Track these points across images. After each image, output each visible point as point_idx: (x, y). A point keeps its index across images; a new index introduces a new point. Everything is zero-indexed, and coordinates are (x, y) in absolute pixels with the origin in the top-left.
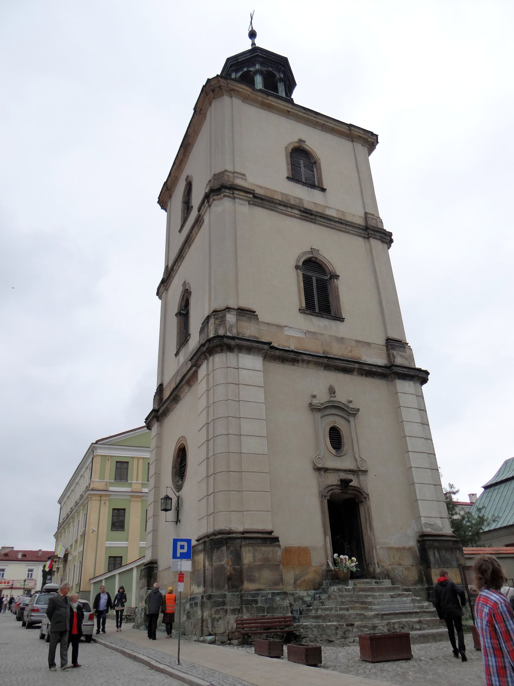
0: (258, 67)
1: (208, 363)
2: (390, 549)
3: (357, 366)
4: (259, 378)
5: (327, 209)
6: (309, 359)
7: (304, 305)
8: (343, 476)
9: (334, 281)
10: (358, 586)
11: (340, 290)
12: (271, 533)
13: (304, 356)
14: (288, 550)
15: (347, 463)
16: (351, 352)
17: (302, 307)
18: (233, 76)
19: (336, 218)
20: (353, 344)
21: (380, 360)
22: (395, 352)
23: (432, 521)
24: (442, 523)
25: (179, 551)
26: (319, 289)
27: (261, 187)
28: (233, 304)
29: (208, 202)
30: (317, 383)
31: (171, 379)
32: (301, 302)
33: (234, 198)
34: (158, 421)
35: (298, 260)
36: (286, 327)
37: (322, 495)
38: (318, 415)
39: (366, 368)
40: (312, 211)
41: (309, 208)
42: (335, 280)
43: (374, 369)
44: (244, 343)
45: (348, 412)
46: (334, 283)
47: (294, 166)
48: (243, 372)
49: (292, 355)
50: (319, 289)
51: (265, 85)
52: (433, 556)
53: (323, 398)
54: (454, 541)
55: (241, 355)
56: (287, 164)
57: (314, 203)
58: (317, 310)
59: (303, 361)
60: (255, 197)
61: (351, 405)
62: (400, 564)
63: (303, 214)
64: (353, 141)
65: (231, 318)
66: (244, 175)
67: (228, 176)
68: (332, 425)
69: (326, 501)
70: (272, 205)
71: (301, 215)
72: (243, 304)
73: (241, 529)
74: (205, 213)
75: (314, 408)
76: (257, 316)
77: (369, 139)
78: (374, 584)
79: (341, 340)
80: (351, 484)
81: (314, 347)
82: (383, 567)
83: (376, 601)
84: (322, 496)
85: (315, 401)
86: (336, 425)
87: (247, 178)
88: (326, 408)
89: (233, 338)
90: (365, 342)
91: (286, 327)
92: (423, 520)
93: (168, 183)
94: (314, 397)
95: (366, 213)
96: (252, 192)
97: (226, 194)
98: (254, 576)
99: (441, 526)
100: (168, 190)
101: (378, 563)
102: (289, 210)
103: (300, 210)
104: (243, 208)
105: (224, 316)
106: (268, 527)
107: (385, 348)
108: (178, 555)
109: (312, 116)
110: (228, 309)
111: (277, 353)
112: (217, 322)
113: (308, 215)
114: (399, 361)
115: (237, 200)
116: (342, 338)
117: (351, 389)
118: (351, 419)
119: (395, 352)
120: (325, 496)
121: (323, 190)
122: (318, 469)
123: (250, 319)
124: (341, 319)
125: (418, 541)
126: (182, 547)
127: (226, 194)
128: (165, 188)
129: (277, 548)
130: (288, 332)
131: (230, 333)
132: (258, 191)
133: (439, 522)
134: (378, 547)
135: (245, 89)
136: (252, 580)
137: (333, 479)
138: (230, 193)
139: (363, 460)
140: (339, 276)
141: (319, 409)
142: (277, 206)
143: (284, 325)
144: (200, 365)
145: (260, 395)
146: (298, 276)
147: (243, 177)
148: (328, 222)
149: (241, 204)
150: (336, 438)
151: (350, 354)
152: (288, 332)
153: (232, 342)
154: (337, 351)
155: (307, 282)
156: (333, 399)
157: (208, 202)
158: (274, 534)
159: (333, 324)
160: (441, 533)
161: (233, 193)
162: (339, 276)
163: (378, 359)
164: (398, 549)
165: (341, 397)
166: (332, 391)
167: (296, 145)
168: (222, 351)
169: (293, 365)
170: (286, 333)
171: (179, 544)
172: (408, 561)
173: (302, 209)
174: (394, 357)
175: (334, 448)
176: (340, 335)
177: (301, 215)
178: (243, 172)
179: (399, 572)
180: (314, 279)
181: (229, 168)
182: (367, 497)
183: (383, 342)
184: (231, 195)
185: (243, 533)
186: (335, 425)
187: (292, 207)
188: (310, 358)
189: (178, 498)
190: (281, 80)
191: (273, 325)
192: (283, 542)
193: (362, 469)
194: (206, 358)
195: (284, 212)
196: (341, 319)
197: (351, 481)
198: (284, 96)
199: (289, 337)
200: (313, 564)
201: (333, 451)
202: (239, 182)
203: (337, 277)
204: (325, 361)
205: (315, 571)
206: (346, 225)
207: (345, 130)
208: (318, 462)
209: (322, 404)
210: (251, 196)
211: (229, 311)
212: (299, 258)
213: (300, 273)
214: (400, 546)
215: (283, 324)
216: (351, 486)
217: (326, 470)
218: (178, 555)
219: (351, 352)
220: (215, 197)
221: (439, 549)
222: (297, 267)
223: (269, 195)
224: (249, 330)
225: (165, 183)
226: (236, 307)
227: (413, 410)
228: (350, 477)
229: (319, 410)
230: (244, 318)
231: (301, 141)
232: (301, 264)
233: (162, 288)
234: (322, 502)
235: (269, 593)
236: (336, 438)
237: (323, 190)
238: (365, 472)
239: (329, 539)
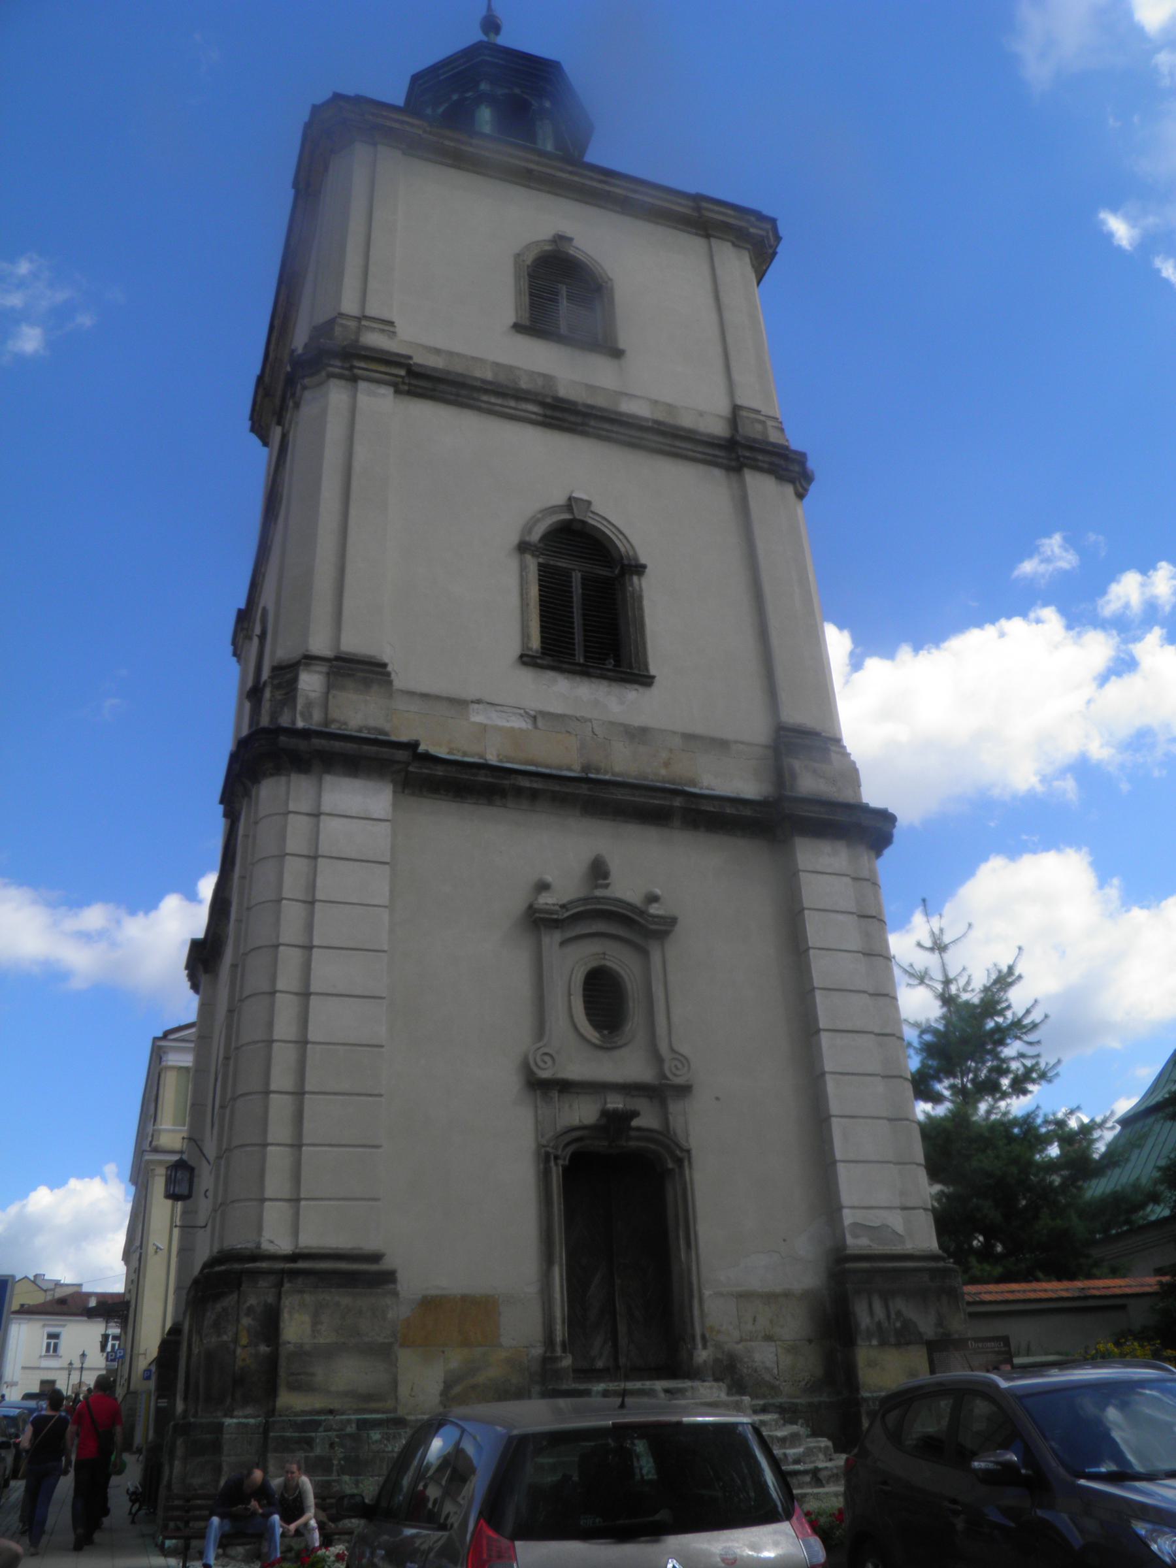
2: (744, 1296)
3: (678, 802)
4: (378, 839)
6: (535, 785)
7: (535, 643)
8: (616, 1103)
9: (631, 580)
11: (646, 603)
12: (376, 1258)
13: (520, 778)
15: (628, 1065)
17: (531, 649)
19: (647, 420)
23: (874, 1219)
26: (585, 603)
27: (437, 351)
28: (320, 645)
32: (525, 635)
33: (354, 379)
35: (528, 528)
36: (478, 702)
37: (547, 1155)
38: (551, 940)
40: (574, 403)
42: (635, 579)
44: (338, 745)
45: (641, 926)
46: (632, 585)
50: (585, 603)
54: (933, 1272)
55: (328, 779)
56: (518, 293)
57: (587, 385)
59: (519, 792)
61: (654, 909)
62: (769, 1338)
63: (549, 412)
64: (708, 236)
65: (310, 683)
66: (391, 323)
68: (594, 964)
70: (463, 392)
71: (545, 416)
72: (353, 643)
76: (388, 674)
77: (752, 230)
78: (662, 1395)
79: (638, 735)
80: (635, 1123)
81: (558, 754)
82: (718, 1346)
84: (545, 1158)
85: (546, 900)
86: (608, 964)
87: (397, 330)
88: (577, 918)
89: (306, 734)
91: (478, 702)
92: (848, 1217)
93: (267, 379)
96: (403, 360)
97: (331, 369)
98: (313, 1375)
99: (900, 1229)
101: (703, 1337)
102: (512, 403)
103: (543, 404)
104: (378, 403)
105: (295, 680)
106: (370, 1244)
109: (591, 179)
111: (440, 771)
112: (279, 695)
113: (562, 415)
114: (808, 784)
117: (647, 865)
119: (797, 764)
120: (556, 1158)
123: (367, 684)
124: (645, 680)
127: (331, 369)
131: (304, 719)
132: (421, 359)
133: (896, 1221)
134: (707, 1293)
135: (408, 123)
136: (301, 1386)
137: (583, 1112)
138: (342, 368)
139: (684, 1060)
140: (644, 567)
141: (556, 921)
142: (475, 395)
143: (470, 698)
145: (378, 886)
147: (386, 328)
151: (663, 772)
152: (478, 716)
153: (302, 745)
154: (623, 762)
156: (599, 893)
157: (293, 395)
158: (385, 1265)
159: (632, 694)
160: (898, 1249)
161: (352, 367)
162: (644, 567)
163: (740, 782)
164: (770, 1298)
165: (625, 887)
166: (598, 871)
167: (548, 248)
168: (278, 771)
169: (490, 803)
172: (794, 1325)
173: (549, 400)
174: (793, 776)
175: (597, 1025)
176: (637, 721)
178: (386, 315)
179: (765, 1357)
180: (577, 577)
184: (346, 372)
185: (294, 1257)
186: (603, 962)
187: (521, 396)
188: (538, 785)
191: (438, 698)
195: (497, 408)
196: (645, 680)
197: (635, 1114)
199: (484, 728)
202: (374, 339)
203: (640, 569)
204: (584, 790)
207: (684, 208)
208: (541, 1064)
209: (563, 906)
210: (403, 373)
211: (307, 665)
213: (532, 564)
214: (778, 1289)
215: (471, 693)
216: (639, 1129)
217: (565, 1087)
219: (667, 764)
220: (307, 381)
222: (523, 547)
223: (458, 367)
224: (358, 712)
226: (327, 652)
227: (841, 917)
228: (641, 1104)
232: (535, 537)
235: (349, 1421)
236: (605, 1000)
237: (617, 353)
238: (684, 1090)
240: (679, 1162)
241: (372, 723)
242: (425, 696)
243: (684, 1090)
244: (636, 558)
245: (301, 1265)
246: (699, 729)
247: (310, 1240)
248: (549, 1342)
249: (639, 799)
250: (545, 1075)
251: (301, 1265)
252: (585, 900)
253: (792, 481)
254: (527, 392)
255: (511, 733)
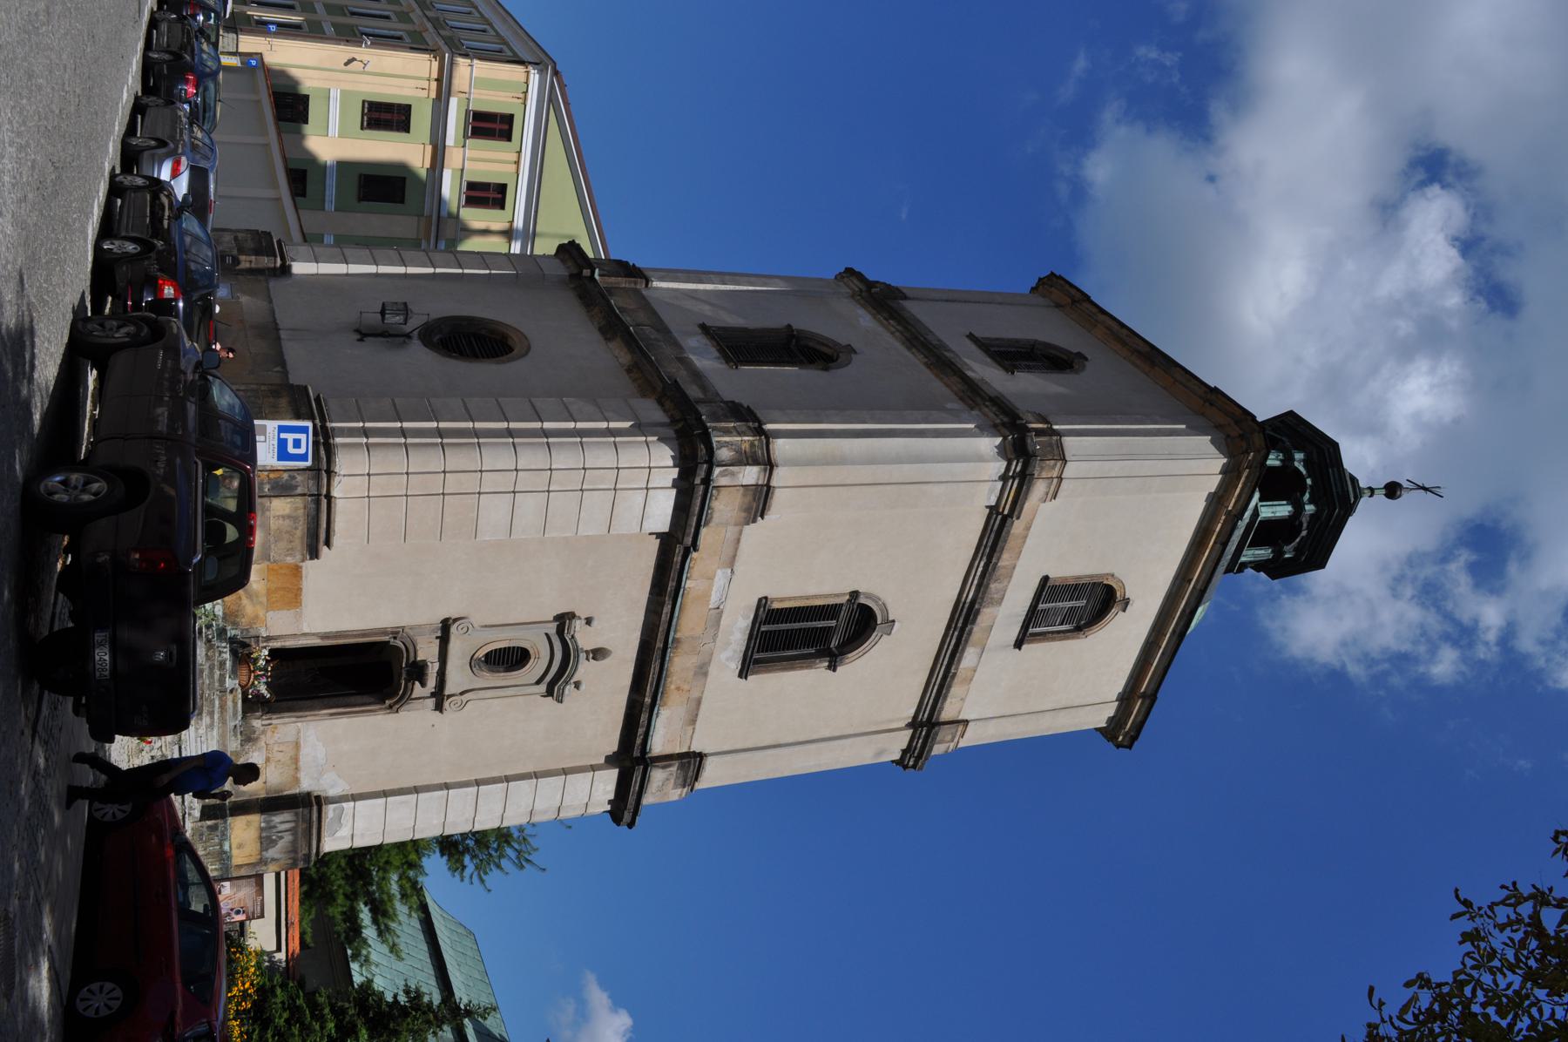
0: (1310, 508)
1: (662, 425)
2: (297, 745)
4: (627, 523)
7: (776, 606)
8: (433, 669)
10: (230, 697)
12: (328, 543)
14: (296, 571)
15: (458, 677)
16: (678, 689)
18: (1299, 456)
20: (695, 694)
21: (660, 743)
22: (674, 769)
24: (343, 838)
25: (290, 437)
27: (1028, 528)
29: (1004, 424)
30: (617, 628)
31: (654, 313)
32: (782, 600)
34: (571, 276)
35: (869, 596)
38: (552, 629)
39: (644, 718)
40: (974, 622)
41: (980, 618)
43: (641, 731)
45: (556, 684)
47: (1073, 589)
48: (639, 497)
51: (1268, 523)
52: (283, 820)
53: (584, 638)
56: (1079, 578)
58: (763, 628)
60: (1005, 519)
61: (570, 689)
65: (751, 475)
67: (1053, 467)
69: (386, 638)
72: (779, 499)
73: (335, 493)
74: (985, 415)
75: (563, 621)
76: (754, 521)
79: (702, 671)
81: (689, 622)
82: (264, 732)
83: (201, 731)
84: (395, 633)
85: (578, 625)
89: (707, 481)
93: (1086, 305)
94: (589, 621)
95: (966, 722)
100: (1074, 302)
105: (756, 462)
106: (336, 540)
107: (685, 750)
108: (283, 436)
110: (769, 465)
111: (678, 559)
113: (963, 619)
114: (657, 776)
115: (1000, 484)
116: (706, 674)
118: (543, 688)
119: (674, 769)
121: (1018, 644)
122: (446, 625)
123: (748, 510)
124: (744, 673)
125: (309, 794)
126: (297, 443)
128: (1078, 295)
129: (299, 557)
130: (721, 576)
132: (1017, 527)
133: (345, 832)
137: (427, 651)
144: (660, 403)
145: (592, 526)
146: (837, 595)
149: (991, 491)
150: (509, 659)
152: (721, 576)
154: (680, 664)
155: (829, 611)
156: (583, 656)
157: (1004, 424)
161: (1014, 478)
165: (585, 670)
166: (598, 654)
170: (719, 572)
171: (302, 437)
174: (664, 767)
175: (487, 655)
176: (713, 670)
180: (833, 623)
181: (1071, 470)
183: (696, 748)
185: (329, 497)
187: (982, 586)
189: (408, 336)
190: (1278, 553)
192: (310, 567)
193: (446, 704)
194: (673, 421)
196: (744, 673)
197: (423, 685)
198: (1243, 559)
199: (711, 578)
201: (481, 654)
202: (1039, 488)
205: (257, 617)
212: (876, 599)
214: (301, 763)
215: (738, 567)
217: (444, 640)
218: (283, 436)
221: (293, 831)
223: (1011, 543)
224: (724, 507)
225: (1087, 298)
226: (773, 483)
229: (560, 632)
230: (749, 498)
231: (1126, 603)
232: (862, 600)
233: (856, 284)
234: (384, 632)
236: (509, 659)
237: (1018, 644)
238: (439, 707)
239: (317, 642)
240: (391, 707)
241: (716, 515)
242: (738, 541)
243: (439, 707)
244: (842, 663)
245: (324, 502)
246: (703, 707)
247: (340, 507)
248: (269, 639)
249: (652, 677)
250: (453, 629)
251: (324, 502)
252: (577, 650)
253: (902, 758)
254: (987, 586)
255: (707, 595)
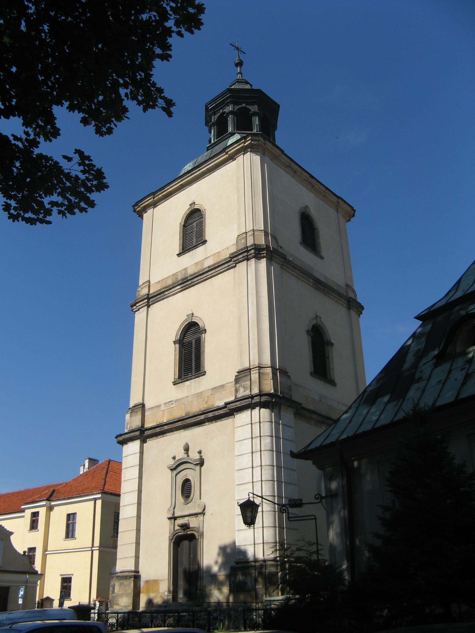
5: (206, 260)
7: (177, 377)
49: (158, 430)
63: (182, 286)
68: (184, 479)
71: (182, 287)
79: (199, 395)
84: (171, 540)
90: (220, 386)
116: (201, 393)
142: (165, 294)
148: (202, 277)
150: (186, 489)
151: (205, 406)
154: (196, 407)
177: (182, 287)
182: (202, 535)
191: (155, 407)
200: (160, 591)
206: (215, 268)
213: (177, 346)
223: (164, 285)
236: (186, 489)
